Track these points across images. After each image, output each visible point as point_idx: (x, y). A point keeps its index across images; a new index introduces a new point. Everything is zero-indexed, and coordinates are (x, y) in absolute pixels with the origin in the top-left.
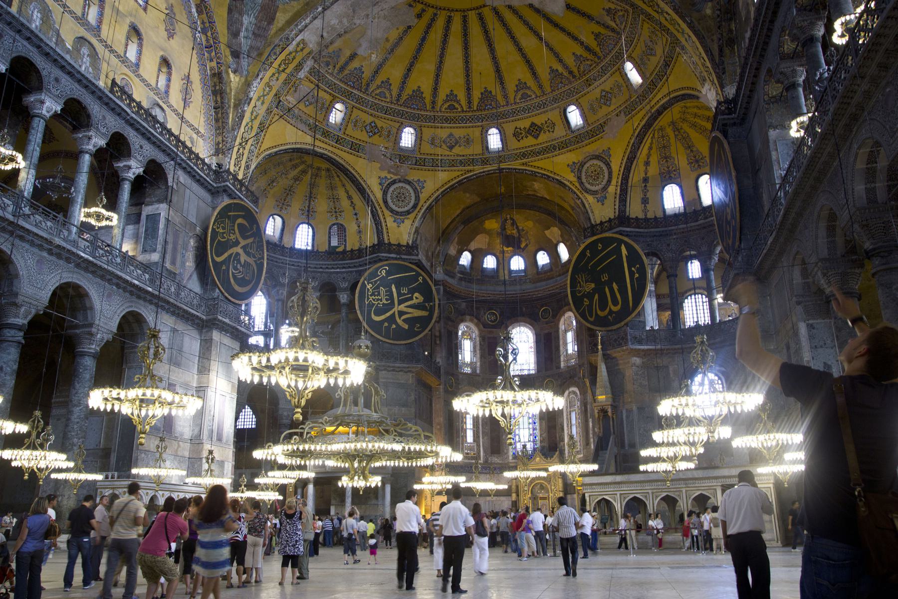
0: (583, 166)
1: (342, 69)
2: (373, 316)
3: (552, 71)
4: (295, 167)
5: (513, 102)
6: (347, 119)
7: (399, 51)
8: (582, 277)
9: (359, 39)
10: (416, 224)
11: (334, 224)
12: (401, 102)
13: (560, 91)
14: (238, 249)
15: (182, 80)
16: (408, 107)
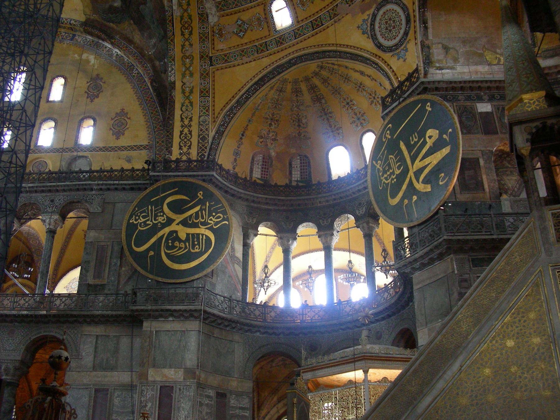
4: (297, 92)
10: (419, 39)
14: (174, 227)
15: (112, 119)
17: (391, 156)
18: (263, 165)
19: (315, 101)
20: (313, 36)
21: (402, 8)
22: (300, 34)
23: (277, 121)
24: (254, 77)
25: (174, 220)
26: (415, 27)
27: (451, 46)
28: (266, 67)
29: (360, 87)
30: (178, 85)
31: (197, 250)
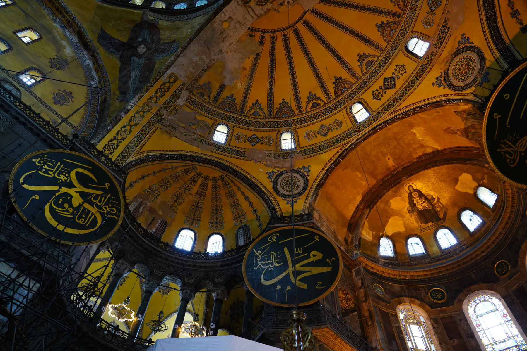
0: (448, 73)
1: (216, 98)
2: (262, 280)
3: (378, 26)
4: (194, 180)
5: (361, 75)
6: (230, 136)
7: (257, 75)
8: (505, 144)
9: (222, 73)
11: (240, 228)
12: (273, 115)
13: (394, 37)
14: (71, 191)
15: (59, 90)
16: (280, 118)
17: (273, 253)
18: (138, 206)
19: (198, 194)
20: (234, 158)
21: (304, 180)
22: (226, 151)
23: (167, 187)
24: (182, 151)
25: (75, 187)
26: (308, 194)
27: (322, 217)
28: (193, 152)
29: (235, 205)
30: (130, 114)
31: (81, 223)
